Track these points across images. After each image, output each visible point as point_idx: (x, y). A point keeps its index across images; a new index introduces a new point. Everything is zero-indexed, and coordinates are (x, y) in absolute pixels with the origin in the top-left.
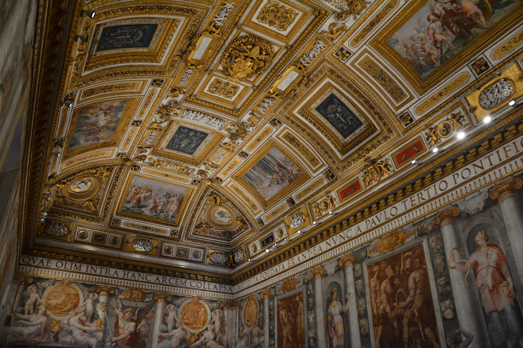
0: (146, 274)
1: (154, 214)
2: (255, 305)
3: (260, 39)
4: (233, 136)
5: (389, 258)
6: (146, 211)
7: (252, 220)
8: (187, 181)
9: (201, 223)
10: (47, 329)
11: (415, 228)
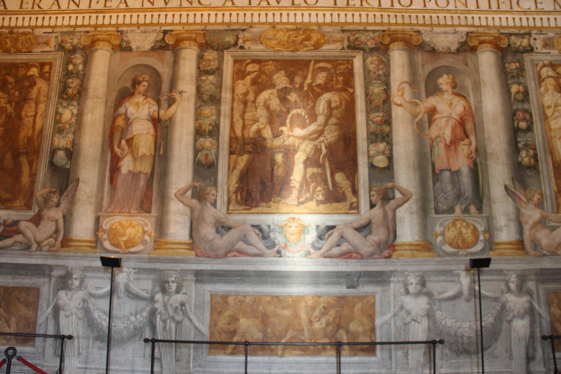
5: (285, 61)
11: (345, 35)
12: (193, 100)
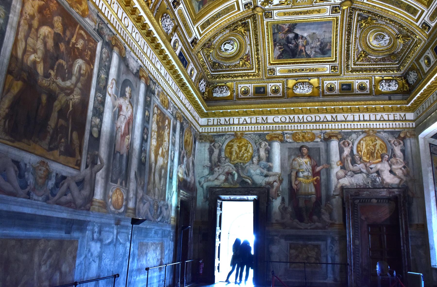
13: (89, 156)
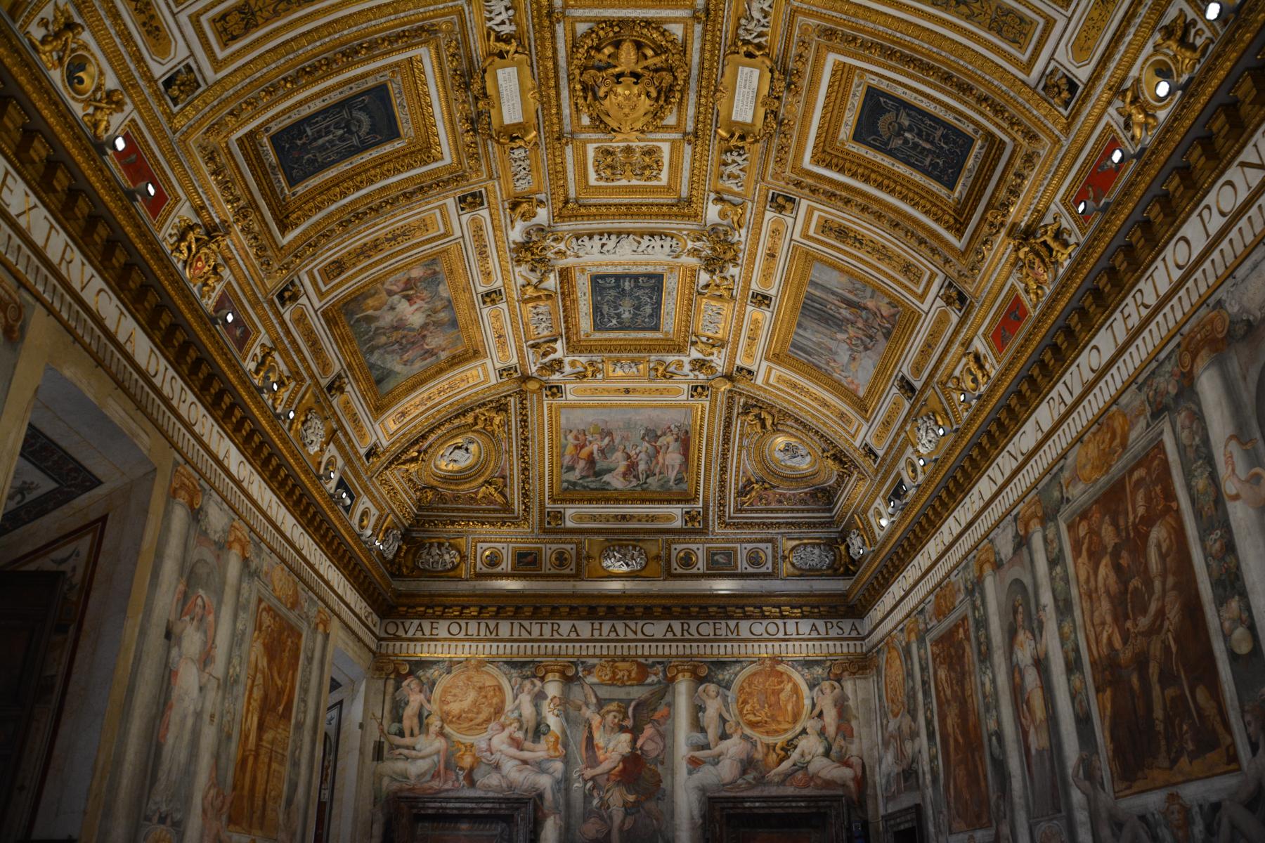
0: (641, 623)
1: (634, 483)
2: (898, 662)
3: (622, 22)
4: (713, 264)
5: (1105, 495)
6: (616, 481)
7: (851, 451)
8: (679, 392)
9: (749, 482)
10: (450, 764)
12: (1054, 616)
13: (1248, 718)
